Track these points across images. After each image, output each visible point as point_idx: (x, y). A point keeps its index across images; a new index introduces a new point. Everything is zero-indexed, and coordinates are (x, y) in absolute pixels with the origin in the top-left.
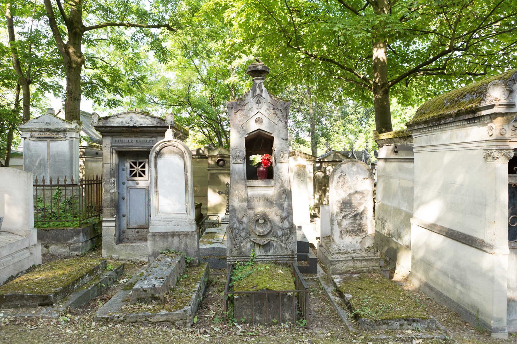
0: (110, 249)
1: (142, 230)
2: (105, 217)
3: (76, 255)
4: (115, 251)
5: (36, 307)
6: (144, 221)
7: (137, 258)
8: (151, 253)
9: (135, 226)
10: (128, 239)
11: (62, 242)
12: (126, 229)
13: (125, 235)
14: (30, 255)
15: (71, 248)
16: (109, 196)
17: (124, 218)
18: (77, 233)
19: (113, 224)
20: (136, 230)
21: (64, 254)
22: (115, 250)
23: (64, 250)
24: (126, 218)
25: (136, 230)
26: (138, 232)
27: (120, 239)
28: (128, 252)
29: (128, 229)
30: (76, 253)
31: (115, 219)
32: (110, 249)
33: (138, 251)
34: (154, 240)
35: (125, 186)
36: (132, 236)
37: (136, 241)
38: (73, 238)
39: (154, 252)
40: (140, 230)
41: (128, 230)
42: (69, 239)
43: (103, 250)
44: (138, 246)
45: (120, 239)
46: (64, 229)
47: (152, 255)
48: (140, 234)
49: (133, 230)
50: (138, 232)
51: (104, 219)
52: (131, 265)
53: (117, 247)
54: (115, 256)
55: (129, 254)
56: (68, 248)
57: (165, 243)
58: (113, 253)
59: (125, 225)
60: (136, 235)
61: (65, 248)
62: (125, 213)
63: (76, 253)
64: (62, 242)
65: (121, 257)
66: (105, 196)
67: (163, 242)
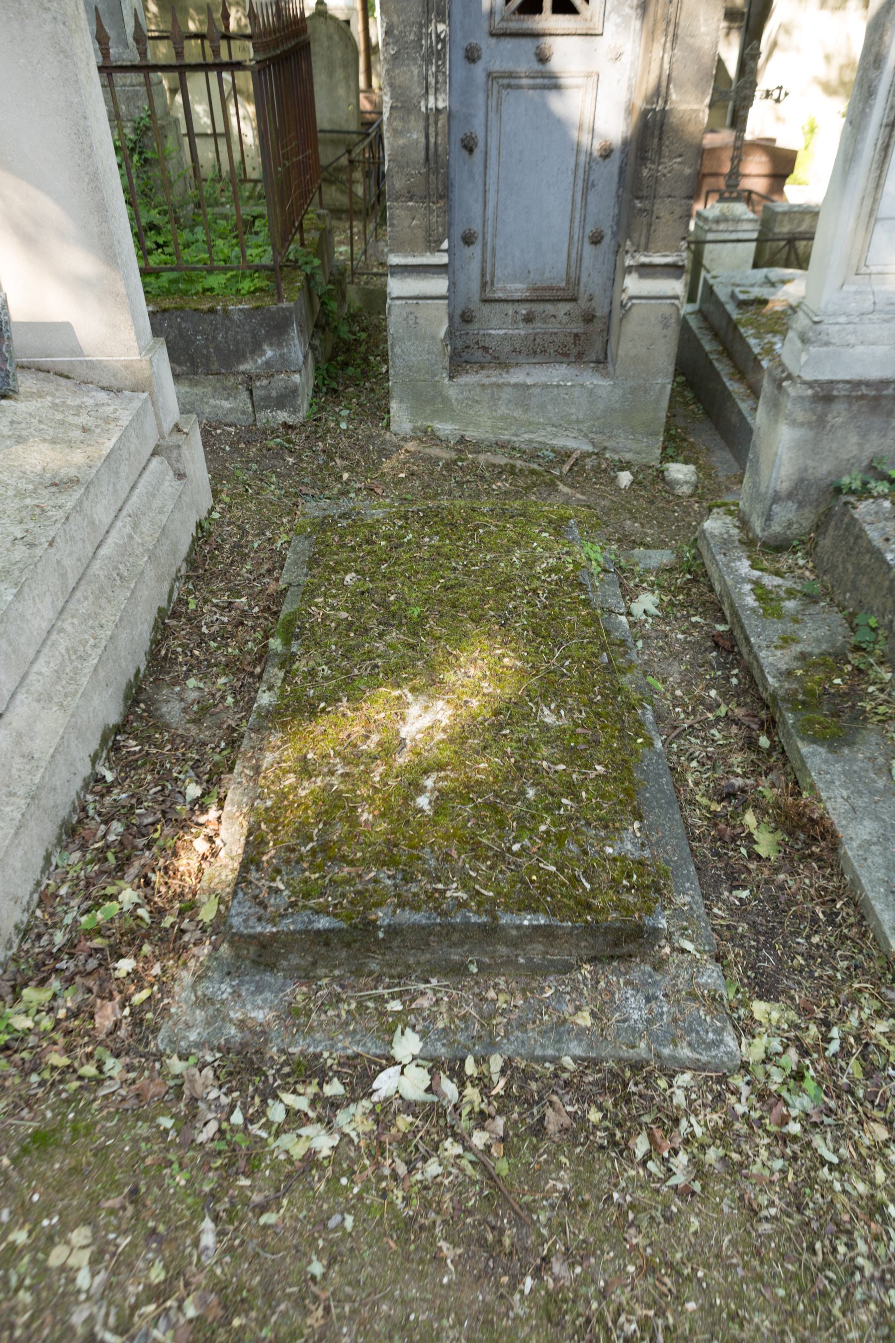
0: (427, 399)
1: (550, 308)
2: (398, 248)
3: (285, 425)
4: (445, 409)
5: (566, 968)
6: (562, 266)
7: (539, 437)
8: (784, 487)
9: (517, 288)
10: (486, 349)
11: (215, 367)
12: (475, 304)
13: (473, 328)
14: (176, 483)
15: (257, 393)
16: (417, 135)
17: (469, 251)
18: (277, 329)
19: (439, 285)
20: (523, 310)
21: (231, 418)
22: (446, 401)
23: (227, 405)
24: (476, 250)
25: (523, 310)
26: (529, 319)
27: (465, 351)
28: (503, 410)
29: (485, 301)
30: (283, 416)
31: (443, 259)
32: (427, 399)
33: (542, 407)
34: (820, 423)
35: (479, 70)
36: (505, 337)
37: (521, 359)
38: (257, 348)
39: (802, 480)
40: (537, 308)
41: (487, 309)
42: (241, 357)
43: (394, 405)
44: (545, 386)
45: (465, 351)
46: (212, 311)
47: (790, 496)
48: (538, 325)
49: (510, 309)
50: (529, 319)
51: (394, 260)
52: (533, 472)
53: (452, 390)
54: (445, 428)
55: (504, 418)
56: (245, 395)
57: (873, 437)
58: (436, 414)
59: (475, 285)
60: (522, 330)
61: (229, 393)
62: (477, 227)
63: (283, 416)
64: (215, 367)
65: (472, 434)
66: (396, 133)
67: (864, 435)
